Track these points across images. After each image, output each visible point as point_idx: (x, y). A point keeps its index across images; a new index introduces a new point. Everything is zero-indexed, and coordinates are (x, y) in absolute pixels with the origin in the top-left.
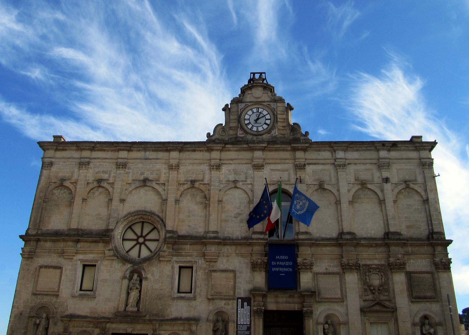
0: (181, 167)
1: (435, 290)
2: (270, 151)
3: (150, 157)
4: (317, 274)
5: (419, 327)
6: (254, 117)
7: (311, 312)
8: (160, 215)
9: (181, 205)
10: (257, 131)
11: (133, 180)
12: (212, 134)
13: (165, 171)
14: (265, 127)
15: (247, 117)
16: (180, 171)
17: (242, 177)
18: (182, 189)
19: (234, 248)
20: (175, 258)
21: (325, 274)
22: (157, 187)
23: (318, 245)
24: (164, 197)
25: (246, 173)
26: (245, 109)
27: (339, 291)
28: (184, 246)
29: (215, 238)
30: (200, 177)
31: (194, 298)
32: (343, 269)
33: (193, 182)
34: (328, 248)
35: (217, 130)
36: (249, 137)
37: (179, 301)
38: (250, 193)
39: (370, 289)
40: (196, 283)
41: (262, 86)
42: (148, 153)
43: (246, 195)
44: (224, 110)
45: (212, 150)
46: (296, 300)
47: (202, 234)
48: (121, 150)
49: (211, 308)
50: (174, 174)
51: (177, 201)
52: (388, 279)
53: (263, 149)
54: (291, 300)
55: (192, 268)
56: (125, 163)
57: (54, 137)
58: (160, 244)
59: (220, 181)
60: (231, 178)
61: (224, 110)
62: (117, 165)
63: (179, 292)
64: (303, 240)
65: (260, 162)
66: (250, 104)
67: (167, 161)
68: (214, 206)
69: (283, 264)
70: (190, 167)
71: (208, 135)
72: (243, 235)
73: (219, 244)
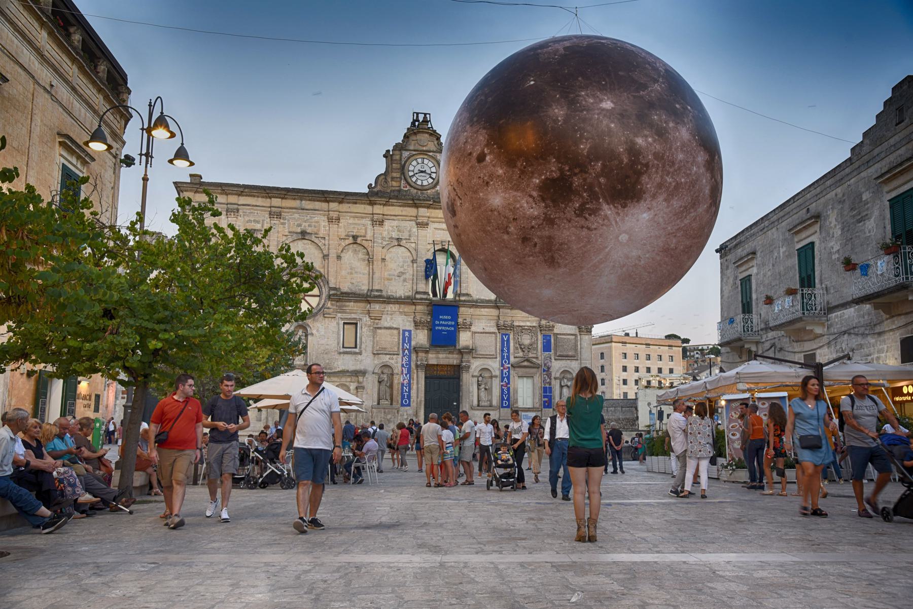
0: (341, 221)
1: (576, 350)
2: (435, 208)
3: (307, 207)
4: (476, 333)
5: (558, 381)
6: (419, 167)
7: (469, 367)
8: (322, 270)
9: (342, 261)
10: (422, 185)
11: (290, 232)
12: (373, 186)
13: (323, 224)
14: (430, 181)
15: (411, 168)
16: (340, 224)
17: (406, 235)
18: (343, 244)
19: (397, 306)
20: (339, 315)
21: (481, 333)
22: (316, 241)
23: (477, 307)
24: (325, 252)
25: (410, 231)
26: (409, 158)
27: (494, 349)
28: (347, 304)
29: (380, 296)
30: (362, 232)
31: (360, 353)
32: (498, 329)
33: (355, 237)
34: (486, 310)
35: (379, 181)
36: (414, 191)
37: (346, 355)
38: (413, 252)
39: (521, 348)
40: (361, 339)
41: (427, 133)
42: (303, 202)
43: (409, 254)
44: (384, 156)
45: (376, 204)
46: (456, 356)
47: (366, 292)
48: (274, 197)
49: (376, 362)
50: (334, 227)
51: (339, 257)
52: (537, 340)
53: (428, 207)
54: (450, 356)
55: (356, 324)
56: (280, 212)
57: (191, 176)
58: (323, 300)
59: (383, 238)
60: (395, 235)
61: (384, 156)
62: (270, 214)
63: (343, 347)
64: (464, 301)
65: (425, 220)
66: (414, 153)
67: (327, 213)
68: (377, 265)
69: (446, 323)
70: (351, 221)
71: (371, 185)
72: (406, 294)
73: (384, 302)
